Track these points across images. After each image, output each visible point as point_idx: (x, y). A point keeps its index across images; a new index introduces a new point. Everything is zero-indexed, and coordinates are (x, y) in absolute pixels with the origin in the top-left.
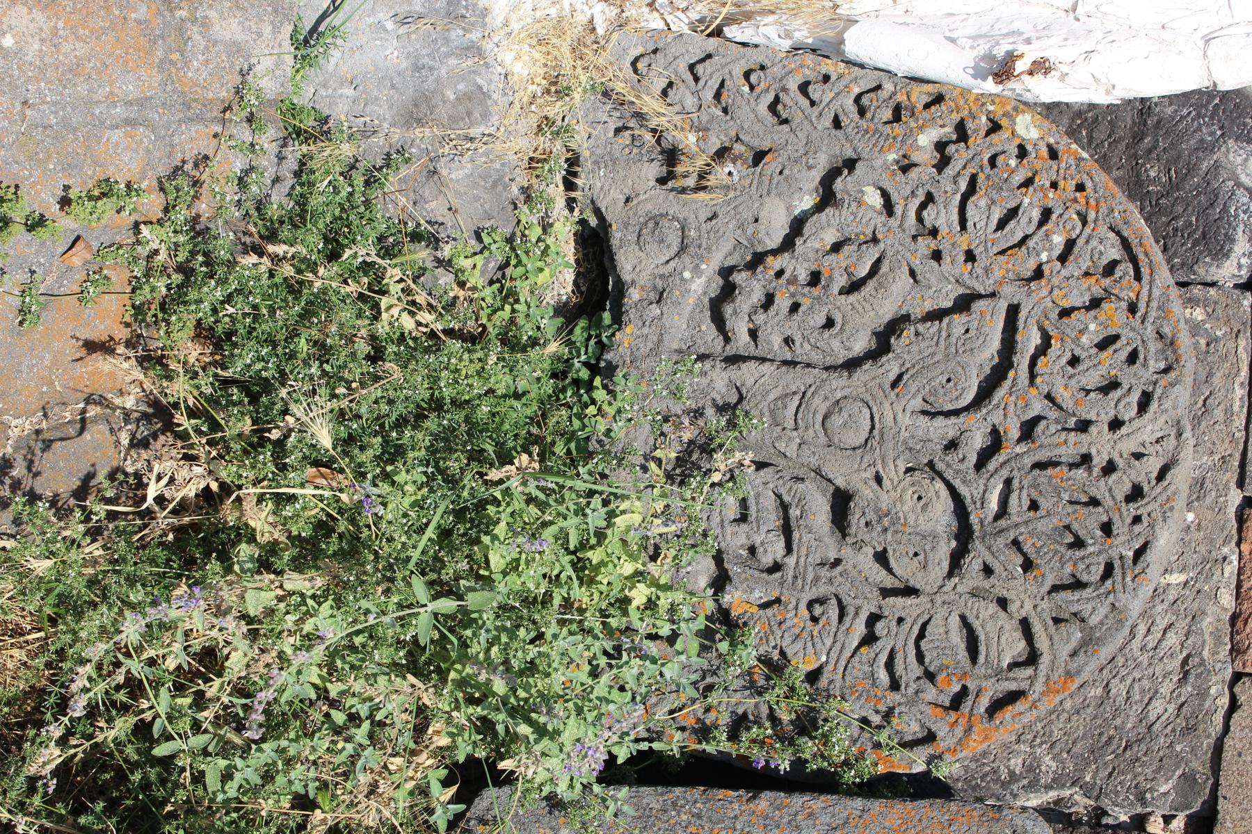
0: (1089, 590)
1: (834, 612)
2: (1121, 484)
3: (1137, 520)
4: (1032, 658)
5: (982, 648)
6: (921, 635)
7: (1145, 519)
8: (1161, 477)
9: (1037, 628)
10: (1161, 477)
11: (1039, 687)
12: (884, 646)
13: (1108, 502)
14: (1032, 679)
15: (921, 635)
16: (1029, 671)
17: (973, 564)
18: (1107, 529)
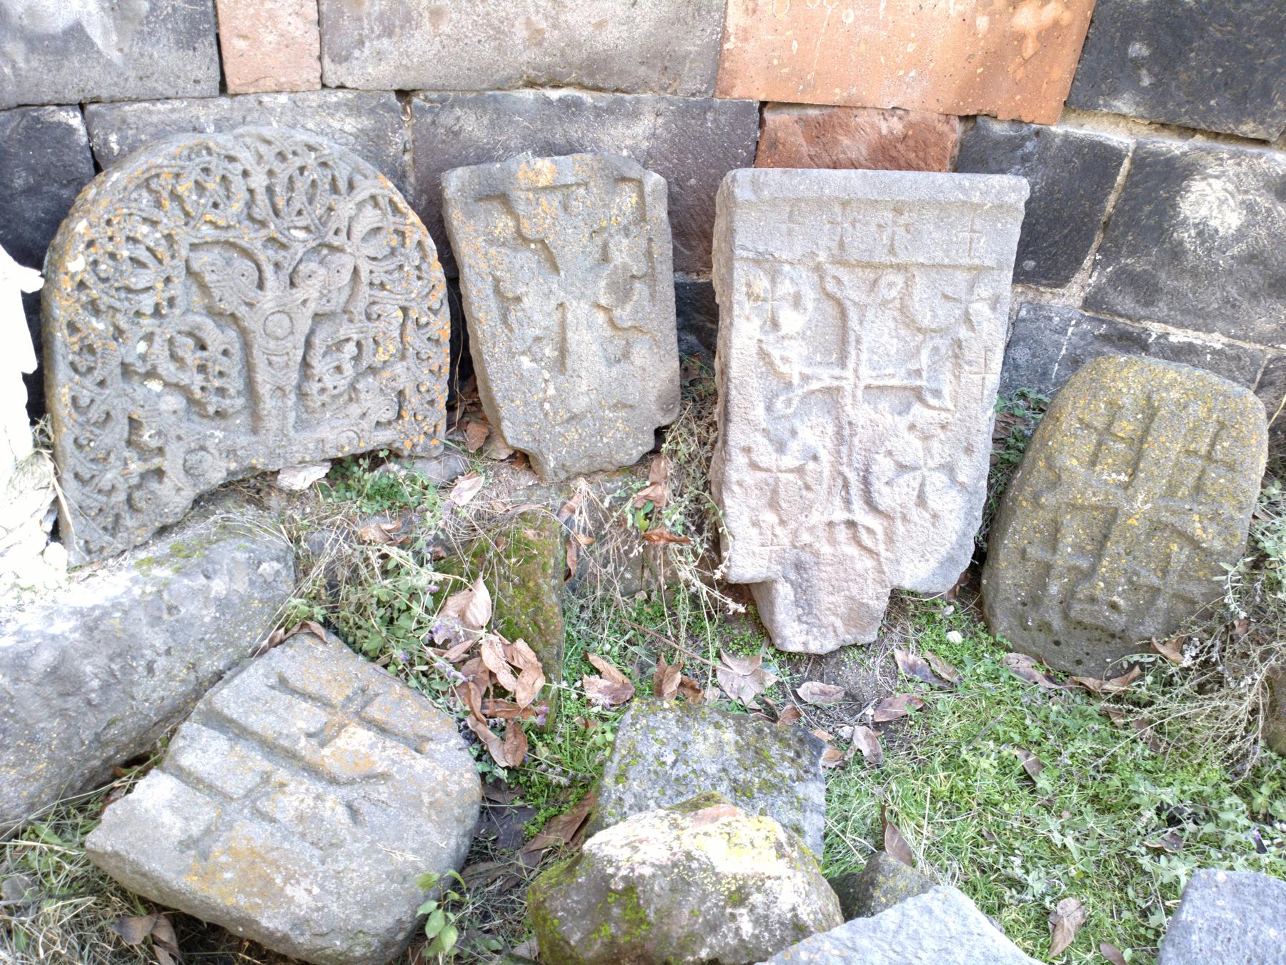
0: (336, 173)
1: (375, 308)
2: (277, 166)
3: (295, 153)
4: (373, 197)
5: (376, 225)
6: (374, 259)
7: (294, 148)
8: (269, 143)
9: (359, 198)
10: (269, 143)
11: (386, 192)
12: (385, 278)
13: (289, 171)
14: (383, 196)
15: (374, 259)
16: (380, 198)
17: (336, 242)
18: (302, 170)
